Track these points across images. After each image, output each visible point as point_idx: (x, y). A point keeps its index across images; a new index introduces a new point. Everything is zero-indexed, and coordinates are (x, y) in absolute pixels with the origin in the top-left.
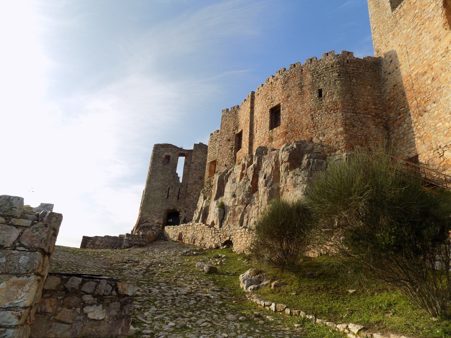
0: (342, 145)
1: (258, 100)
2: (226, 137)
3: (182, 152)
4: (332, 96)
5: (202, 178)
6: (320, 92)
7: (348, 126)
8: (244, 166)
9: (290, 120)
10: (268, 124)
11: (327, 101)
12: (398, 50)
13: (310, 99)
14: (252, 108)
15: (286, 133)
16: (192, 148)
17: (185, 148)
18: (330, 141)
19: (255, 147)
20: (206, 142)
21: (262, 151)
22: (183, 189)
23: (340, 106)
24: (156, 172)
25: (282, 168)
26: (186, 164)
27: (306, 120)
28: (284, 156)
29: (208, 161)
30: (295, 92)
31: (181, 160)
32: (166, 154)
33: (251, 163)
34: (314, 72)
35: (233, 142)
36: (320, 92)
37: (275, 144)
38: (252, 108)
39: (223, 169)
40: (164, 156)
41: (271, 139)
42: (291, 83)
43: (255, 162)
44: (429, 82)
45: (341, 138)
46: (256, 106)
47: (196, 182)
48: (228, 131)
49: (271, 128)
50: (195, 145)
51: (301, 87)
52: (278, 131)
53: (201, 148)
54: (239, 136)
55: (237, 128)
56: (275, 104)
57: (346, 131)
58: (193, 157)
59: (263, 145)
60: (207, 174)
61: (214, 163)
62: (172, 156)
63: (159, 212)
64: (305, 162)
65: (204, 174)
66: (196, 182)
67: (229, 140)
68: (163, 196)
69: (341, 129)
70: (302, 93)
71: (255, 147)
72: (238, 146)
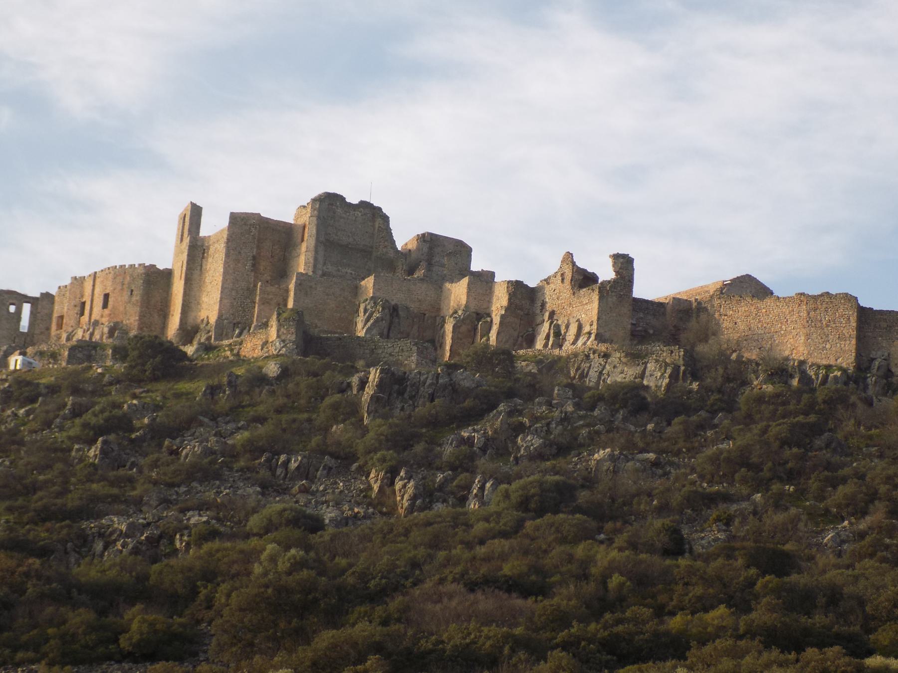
1: (98, 281)
2: (73, 303)
4: (137, 297)
5: (48, 329)
7: (142, 316)
9: (113, 307)
11: (134, 299)
14: (94, 286)
16: (38, 295)
17: (30, 294)
18: (131, 324)
19: (92, 321)
20: (53, 291)
21: (96, 323)
22: (28, 339)
25: (104, 337)
26: (32, 313)
27: (122, 309)
28: (106, 330)
29: (55, 315)
30: (119, 287)
31: (27, 308)
33: (88, 330)
34: (131, 276)
35: (78, 308)
36: (132, 291)
38: (94, 286)
39: (70, 330)
41: (102, 316)
43: (91, 330)
45: (136, 323)
46: (96, 286)
47: (42, 333)
50: (42, 294)
51: (123, 284)
52: (106, 311)
53: (47, 297)
54: (84, 304)
55: (82, 296)
56: (107, 292)
57: (140, 319)
58: (40, 307)
59: (97, 318)
60: (54, 326)
61: (61, 317)
64: (116, 335)
65: (51, 323)
66: (42, 333)
71: (92, 321)
72: (82, 314)
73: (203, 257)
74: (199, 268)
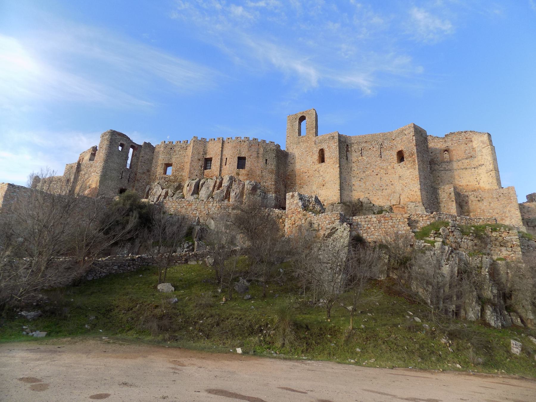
0: (273, 190)
3: (134, 145)
6: (266, 160)
8: (216, 182)
10: (236, 164)
11: (269, 167)
12: (297, 155)
13: (261, 163)
14: (222, 148)
15: (248, 175)
16: (141, 144)
22: (132, 175)
23: (274, 172)
24: (112, 155)
27: (258, 172)
32: (122, 142)
34: (265, 149)
36: (266, 160)
37: (241, 178)
40: (119, 143)
41: (238, 174)
42: (253, 149)
44: (307, 177)
45: (273, 187)
48: (199, 153)
49: (238, 167)
52: (242, 171)
55: (206, 154)
59: (233, 175)
62: (126, 145)
63: (115, 189)
66: (144, 173)
67: (199, 160)
68: (118, 177)
69: (273, 183)
70: (258, 157)
73: (347, 151)
74: (345, 158)
